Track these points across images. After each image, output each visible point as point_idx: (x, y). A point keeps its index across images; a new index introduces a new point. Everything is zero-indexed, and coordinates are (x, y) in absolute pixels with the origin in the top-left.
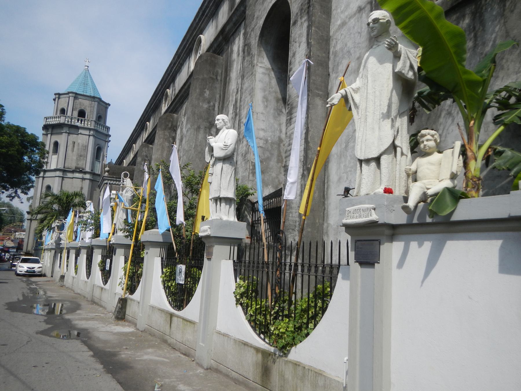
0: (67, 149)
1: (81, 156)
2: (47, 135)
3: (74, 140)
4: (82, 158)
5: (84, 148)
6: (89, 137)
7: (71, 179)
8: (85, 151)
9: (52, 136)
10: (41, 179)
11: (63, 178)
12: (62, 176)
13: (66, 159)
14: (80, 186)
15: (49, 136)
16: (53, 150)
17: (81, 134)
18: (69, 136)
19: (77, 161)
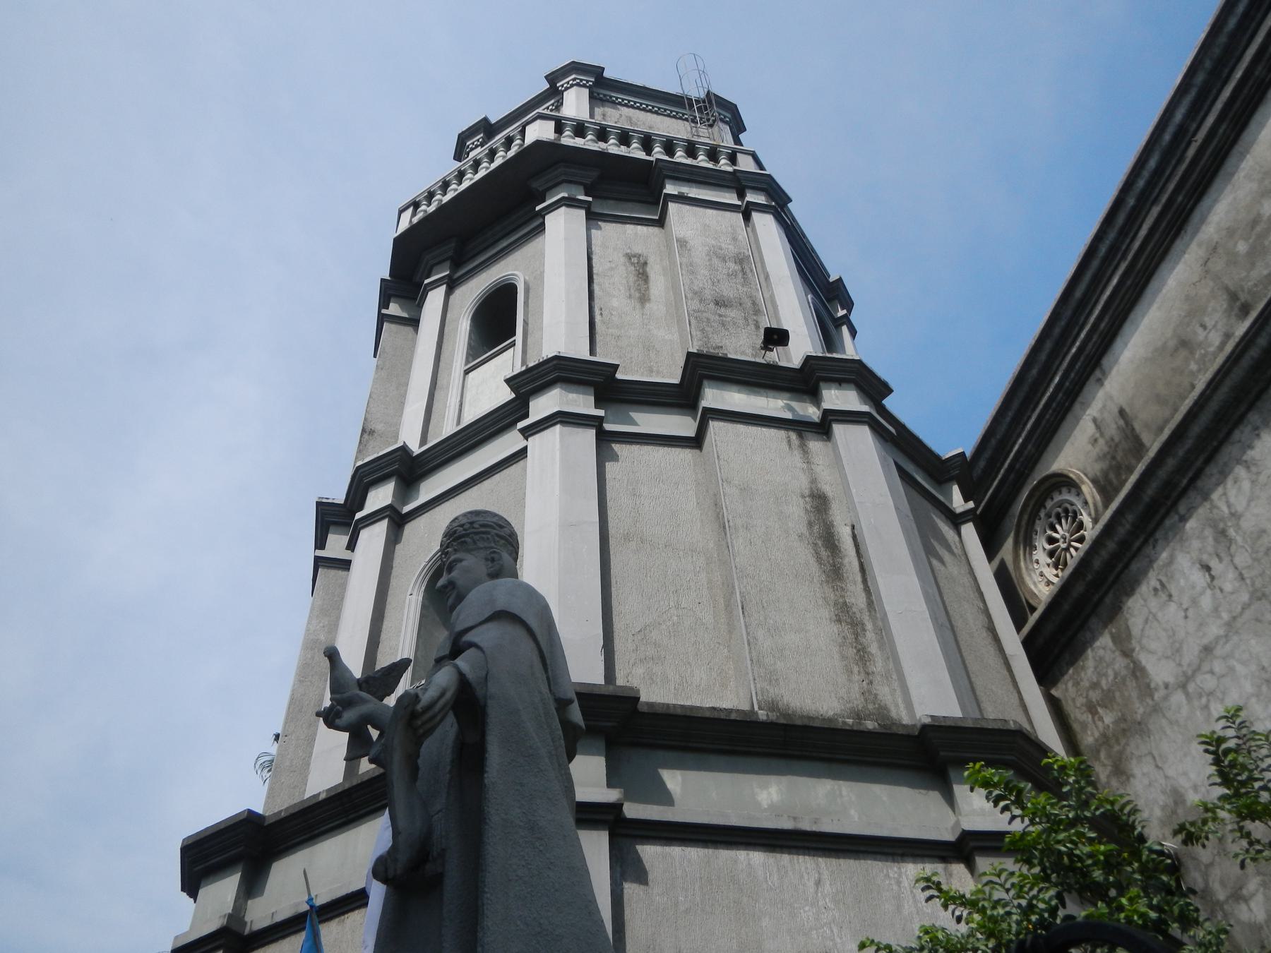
0: (596, 288)
1: (720, 303)
2: (414, 322)
3: (637, 249)
4: (732, 314)
5: (732, 266)
6: (747, 218)
7: (684, 455)
8: (746, 281)
9: (459, 292)
10: (374, 538)
11: (605, 439)
12: (601, 413)
13: (598, 338)
14: (803, 483)
15: (435, 298)
16: (470, 347)
17: (682, 199)
18: (599, 228)
19: (703, 330)
